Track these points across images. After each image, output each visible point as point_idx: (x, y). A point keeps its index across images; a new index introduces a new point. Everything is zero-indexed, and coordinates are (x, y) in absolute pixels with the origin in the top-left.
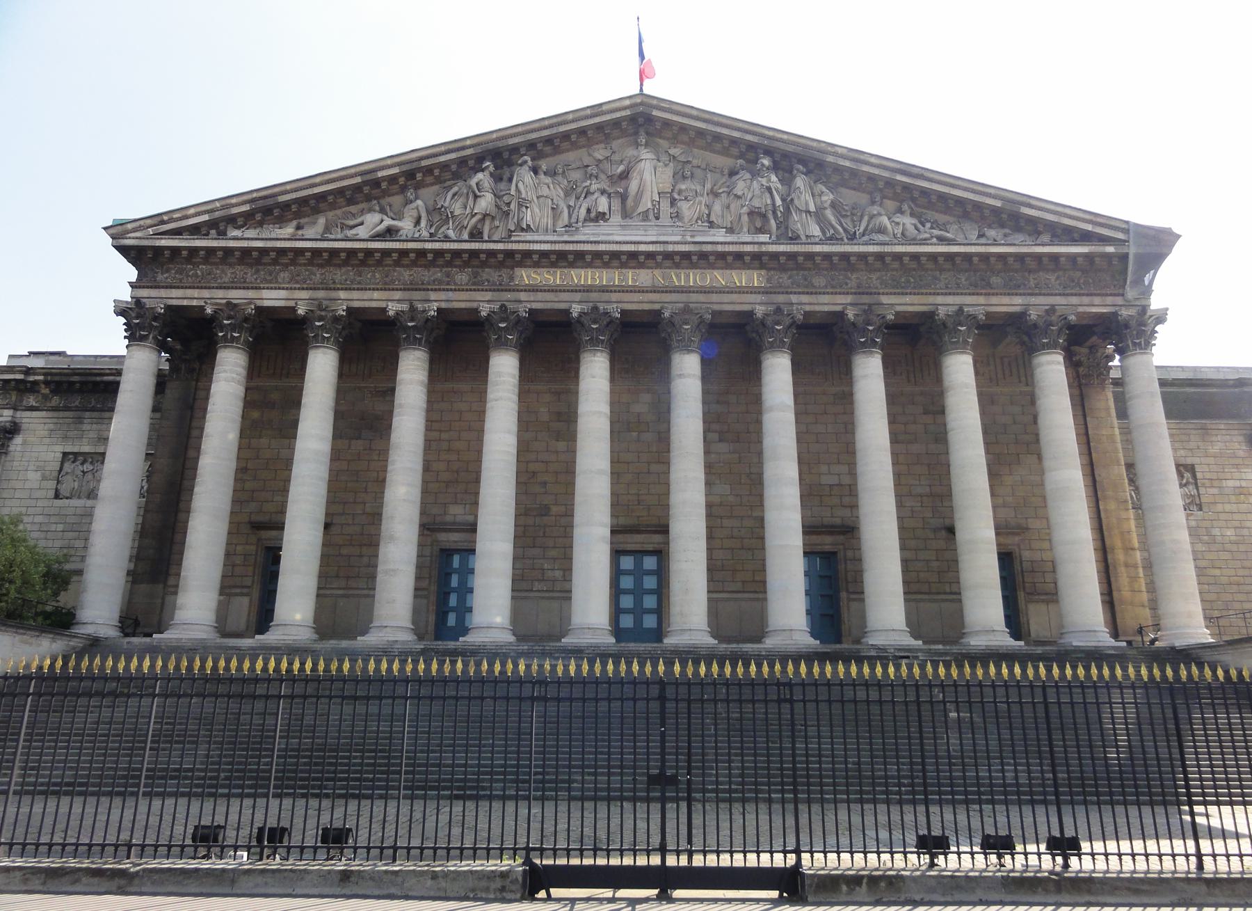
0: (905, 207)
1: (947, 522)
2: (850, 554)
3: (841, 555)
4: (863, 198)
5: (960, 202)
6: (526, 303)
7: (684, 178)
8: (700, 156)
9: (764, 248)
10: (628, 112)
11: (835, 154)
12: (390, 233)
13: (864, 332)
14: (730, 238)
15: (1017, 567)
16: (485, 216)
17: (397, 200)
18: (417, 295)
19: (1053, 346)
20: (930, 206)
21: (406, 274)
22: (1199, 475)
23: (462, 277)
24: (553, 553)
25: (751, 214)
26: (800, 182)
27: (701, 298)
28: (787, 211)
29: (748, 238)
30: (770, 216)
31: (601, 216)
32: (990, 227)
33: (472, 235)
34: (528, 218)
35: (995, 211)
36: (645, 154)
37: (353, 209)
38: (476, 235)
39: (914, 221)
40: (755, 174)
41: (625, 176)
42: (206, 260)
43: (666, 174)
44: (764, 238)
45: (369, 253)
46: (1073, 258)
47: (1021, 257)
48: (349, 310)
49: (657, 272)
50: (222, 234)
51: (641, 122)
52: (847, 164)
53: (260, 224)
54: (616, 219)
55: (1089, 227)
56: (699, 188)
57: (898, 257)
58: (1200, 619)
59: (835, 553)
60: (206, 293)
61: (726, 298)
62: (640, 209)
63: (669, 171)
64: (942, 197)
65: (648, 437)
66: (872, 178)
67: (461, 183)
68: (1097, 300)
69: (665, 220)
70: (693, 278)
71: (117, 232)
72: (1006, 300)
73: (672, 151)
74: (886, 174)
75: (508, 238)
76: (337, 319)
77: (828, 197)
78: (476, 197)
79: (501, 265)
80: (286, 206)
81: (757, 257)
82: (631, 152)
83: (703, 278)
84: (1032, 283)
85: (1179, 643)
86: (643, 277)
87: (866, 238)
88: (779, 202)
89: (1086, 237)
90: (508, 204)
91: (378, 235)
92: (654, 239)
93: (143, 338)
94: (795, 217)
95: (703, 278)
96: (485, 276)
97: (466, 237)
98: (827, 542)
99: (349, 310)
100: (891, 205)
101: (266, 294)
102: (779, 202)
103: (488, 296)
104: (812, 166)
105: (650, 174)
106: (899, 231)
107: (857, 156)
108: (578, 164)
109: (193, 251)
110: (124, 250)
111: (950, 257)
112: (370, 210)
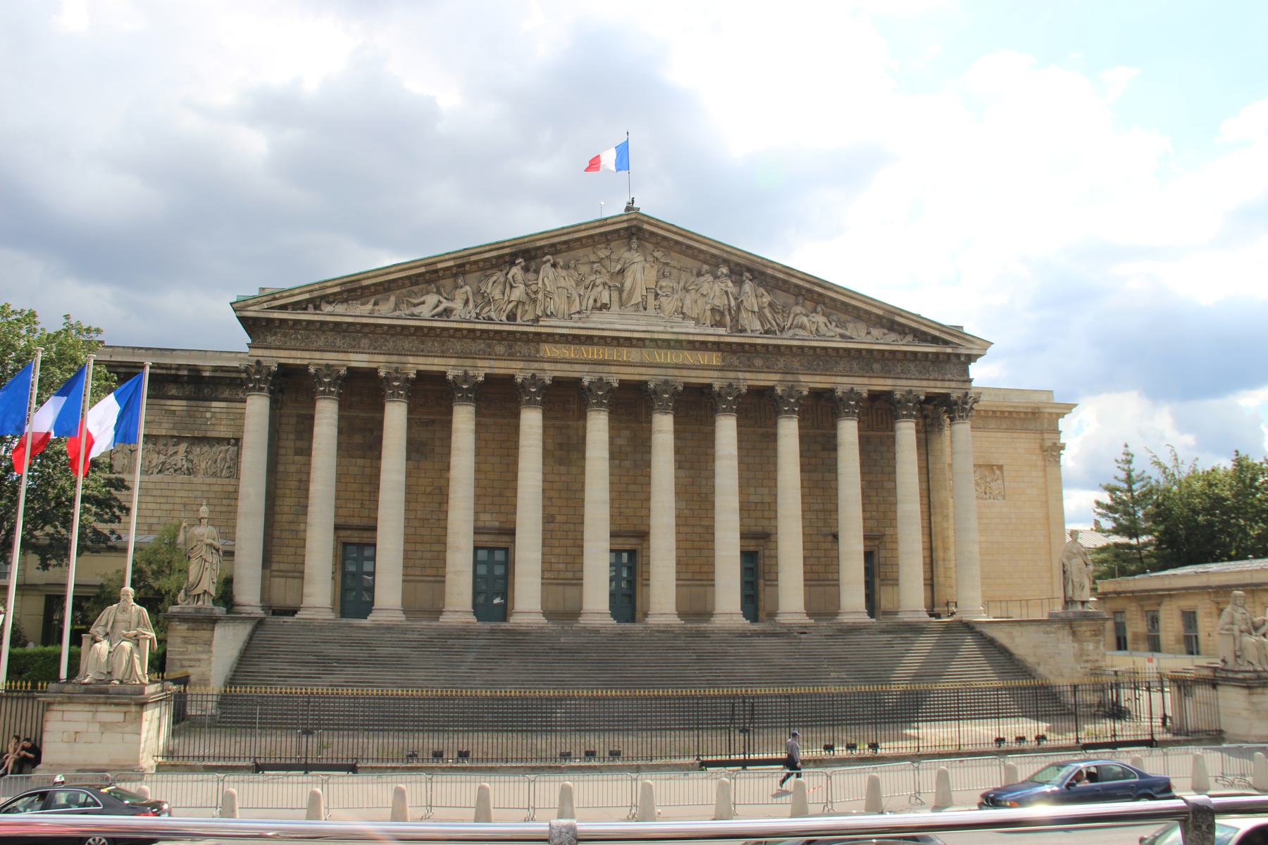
0: (819, 309)
1: (833, 530)
2: (767, 553)
3: (760, 554)
4: (791, 299)
5: (855, 308)
6: (549, 373)
7: (664, 276)
8: (677, 260)
9: (722, 339)
10: (625, 225)
11: (773, 268)
12: (448, 312)
13: (788, 403)
14: (697, 331)
15: (876, 561)
16: (518, 302)
17: (448, 283)
18: (468, 362)
19: (909, 416)
20: (835, 308)
21: (458, 346)
22: (1005, 473)
23: (500, 349)
24: (558, 551)
25: (713, 310)
26: (748, 287)
27: (676, 372)
28: (739, 308)
29: (711, 331)
30: (727, 313)
31: (605, 307)
32: (874, 326)
33: (508, 318)
34: (551, 308)
35: (878, 316)
36: (637, 257)
37: (415, 289)
38: (512, 317)
39: (825, 320)
40: (716, 277)
41: (622, 271)
42: (305, 329)
43: (652, 274)
44: (721, 331)
45: (431, 328)
46: (926, 354)
47: (893, 352)
48: (419, 373)
49: (644, 350)
50: (317, 307)
51: (634, 231)
52: (781, 276)
53: (346, 301)
54: (615, 307)
55: (937, 333)
56: (675, 285)
57: (814, 348)
58: (980, 602)
59: (756, 552)
60: (307, 354)
61: (693, 373)
62: (633, 302)
63: (654, 273)
64: (843, 303)
65: (627, 464)
66: (797, 286)
67: (499, 274)
68: (939, 384)
69: (651, 310)
70: (669, 357)
71: (238, 307)
72: (881, 381)
73: (656, 254)
74: (808, 285)
75: (537, 319)
76: (407, 379)
77: (767, 299)
78: (512, 287)
79: (528, 341)
80: (368, 287)
81: (718, 344)
82: (627, 255)
83: (677, 357)
84: (899, 369)
85: (966, 618)
86: (634, 355)
87: (791, 333)
88: (733, 303)
89: (936, 340)
90: (536, 292)
91: (440, 315)
92: (644, 328)
93: (261, 389)
94: (744, 314)
95: (677, 357)
96: (517, 348)
97: (504, 318)
98: (752, 546)
99: (419, 373)
100: (809, 304)
101: (352, 356)
102: (733, 303)
103: (521, 365)
104: (756, 274)
106: (814, 329)
107: (789, 271)
108: (586, 260)
109: (296, 322)
110: (243, 320)
111: (848, 350)
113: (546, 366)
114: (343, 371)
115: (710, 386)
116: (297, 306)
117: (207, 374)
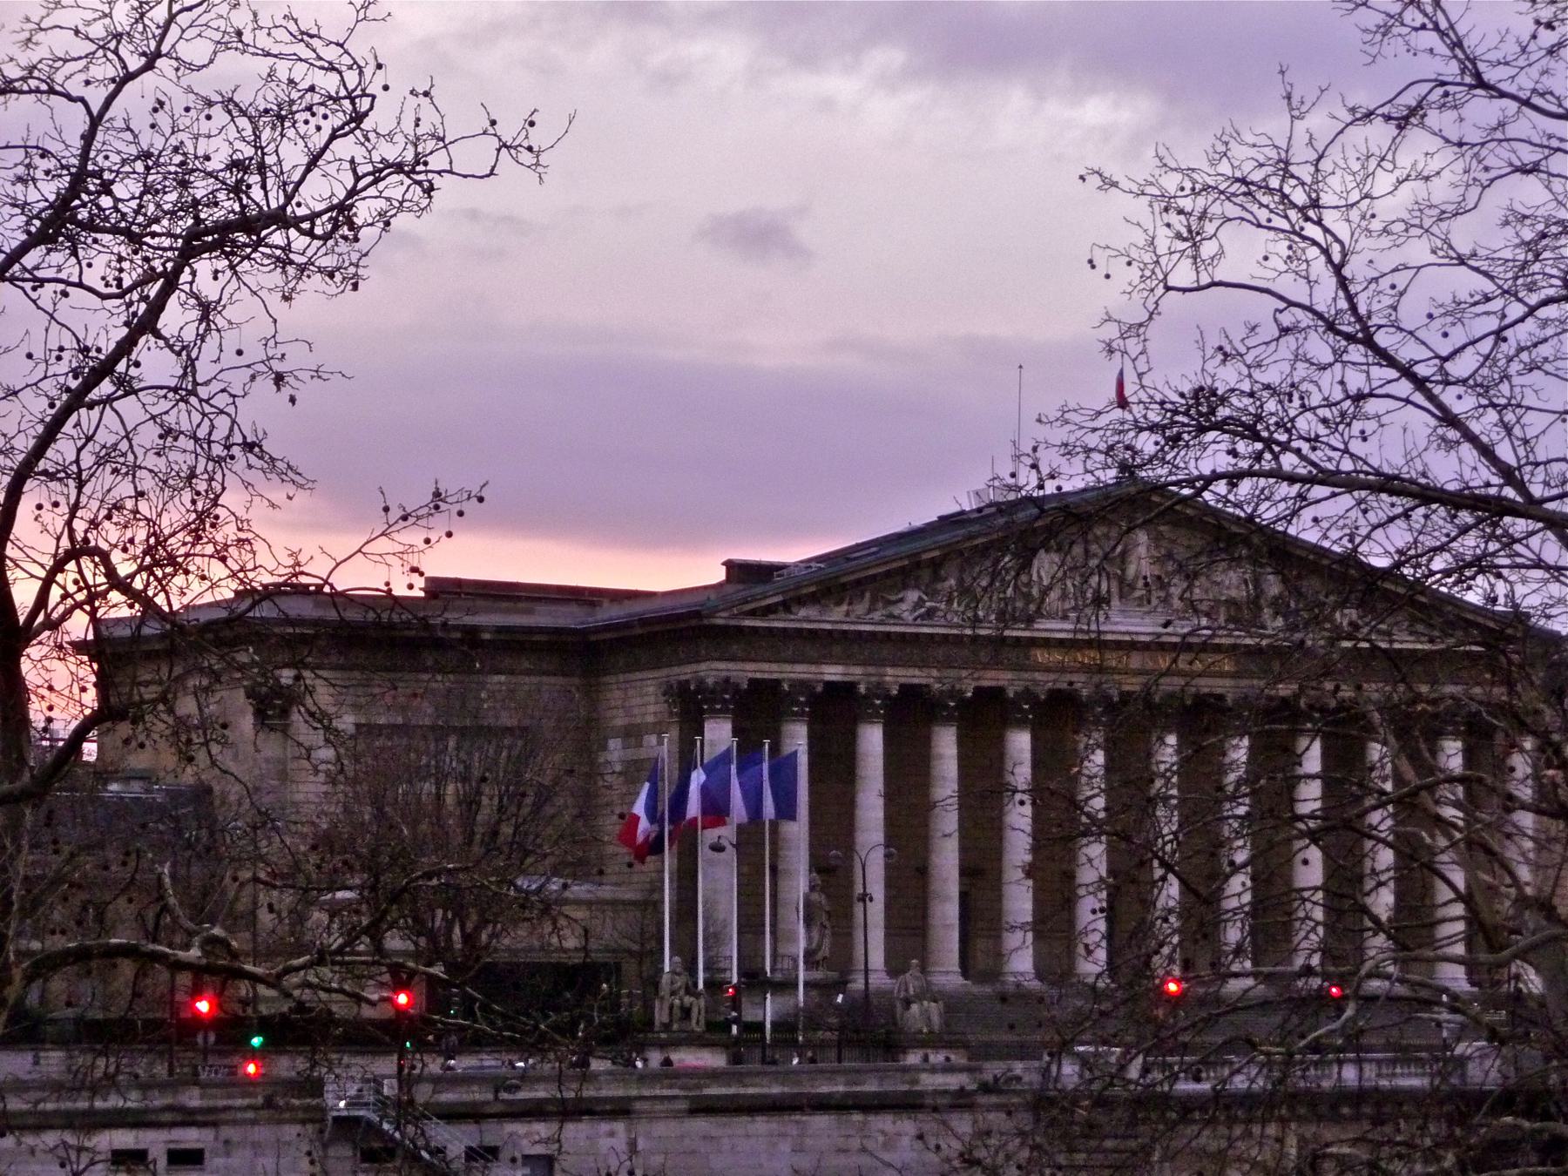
17: (926, 574)
21: (940, 653)
37: (889, 582)
60: (774, 667)
80: (844, 585)
91: (921, 616)
103: (1009, 675)
105: (1142, 557)
112: (905, 587)
113: (1038, 676)
114: (819, 689)
115: (1221, 697)
116: (769, 611)
117: (487, 636)
